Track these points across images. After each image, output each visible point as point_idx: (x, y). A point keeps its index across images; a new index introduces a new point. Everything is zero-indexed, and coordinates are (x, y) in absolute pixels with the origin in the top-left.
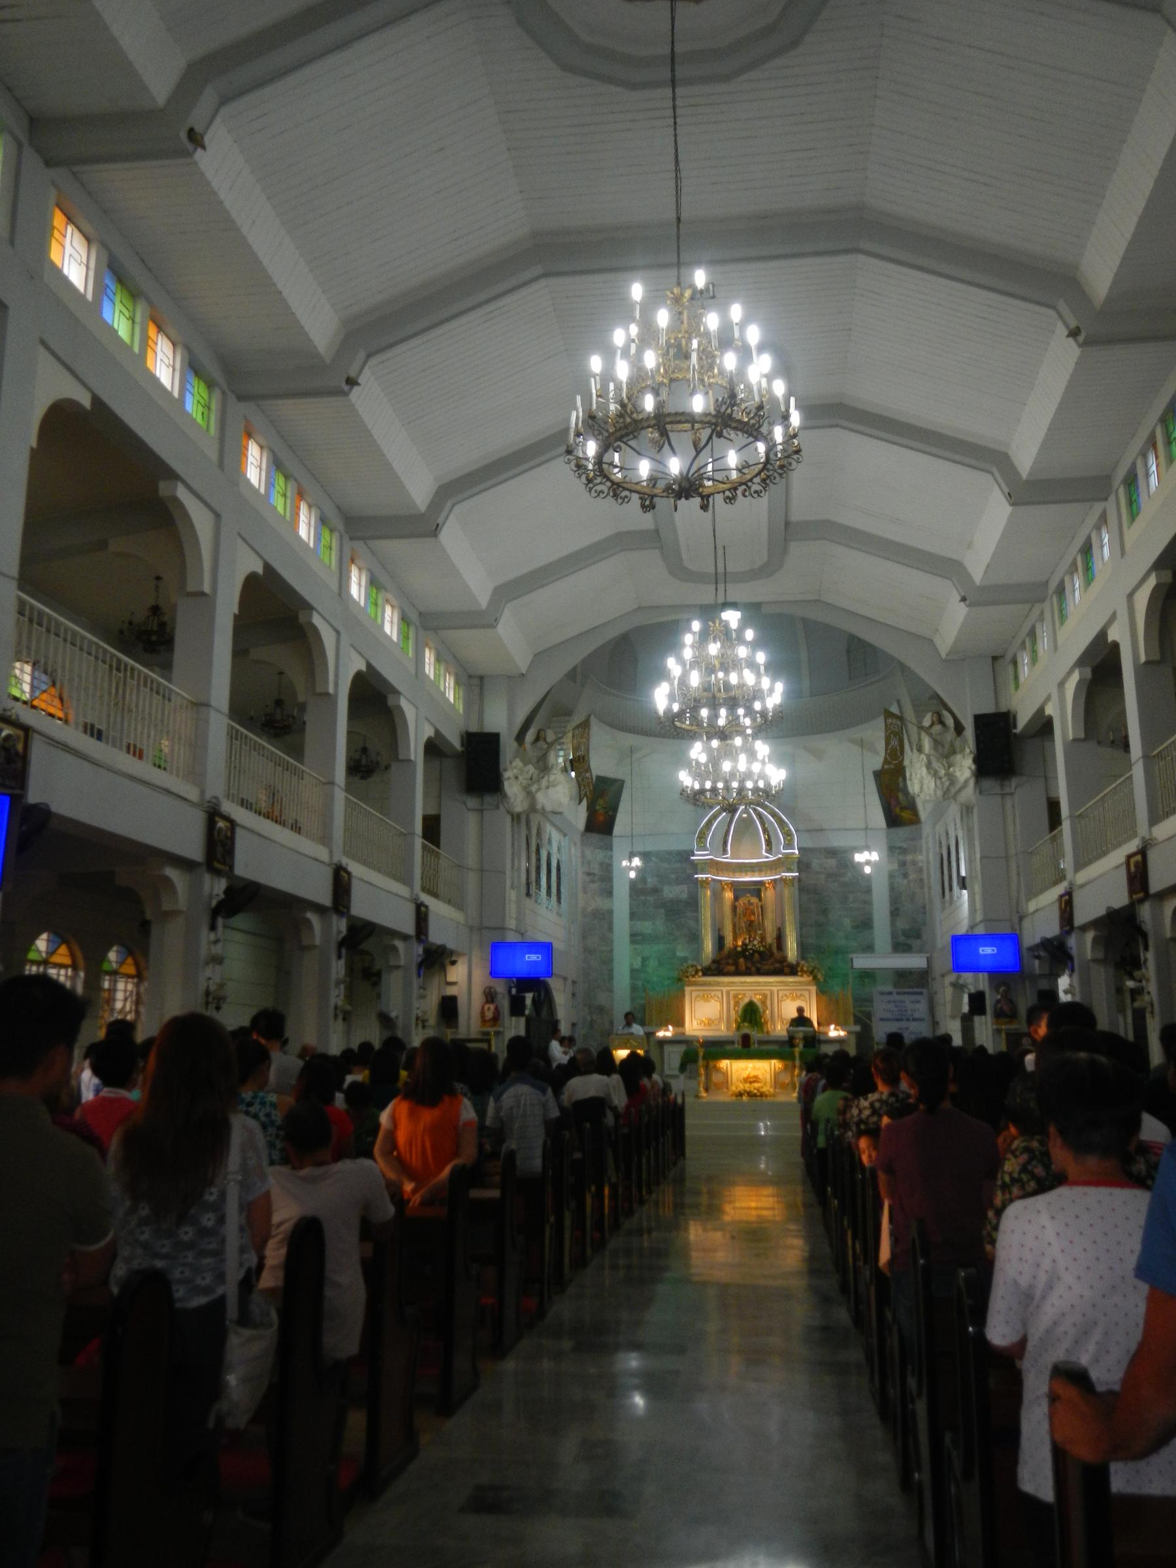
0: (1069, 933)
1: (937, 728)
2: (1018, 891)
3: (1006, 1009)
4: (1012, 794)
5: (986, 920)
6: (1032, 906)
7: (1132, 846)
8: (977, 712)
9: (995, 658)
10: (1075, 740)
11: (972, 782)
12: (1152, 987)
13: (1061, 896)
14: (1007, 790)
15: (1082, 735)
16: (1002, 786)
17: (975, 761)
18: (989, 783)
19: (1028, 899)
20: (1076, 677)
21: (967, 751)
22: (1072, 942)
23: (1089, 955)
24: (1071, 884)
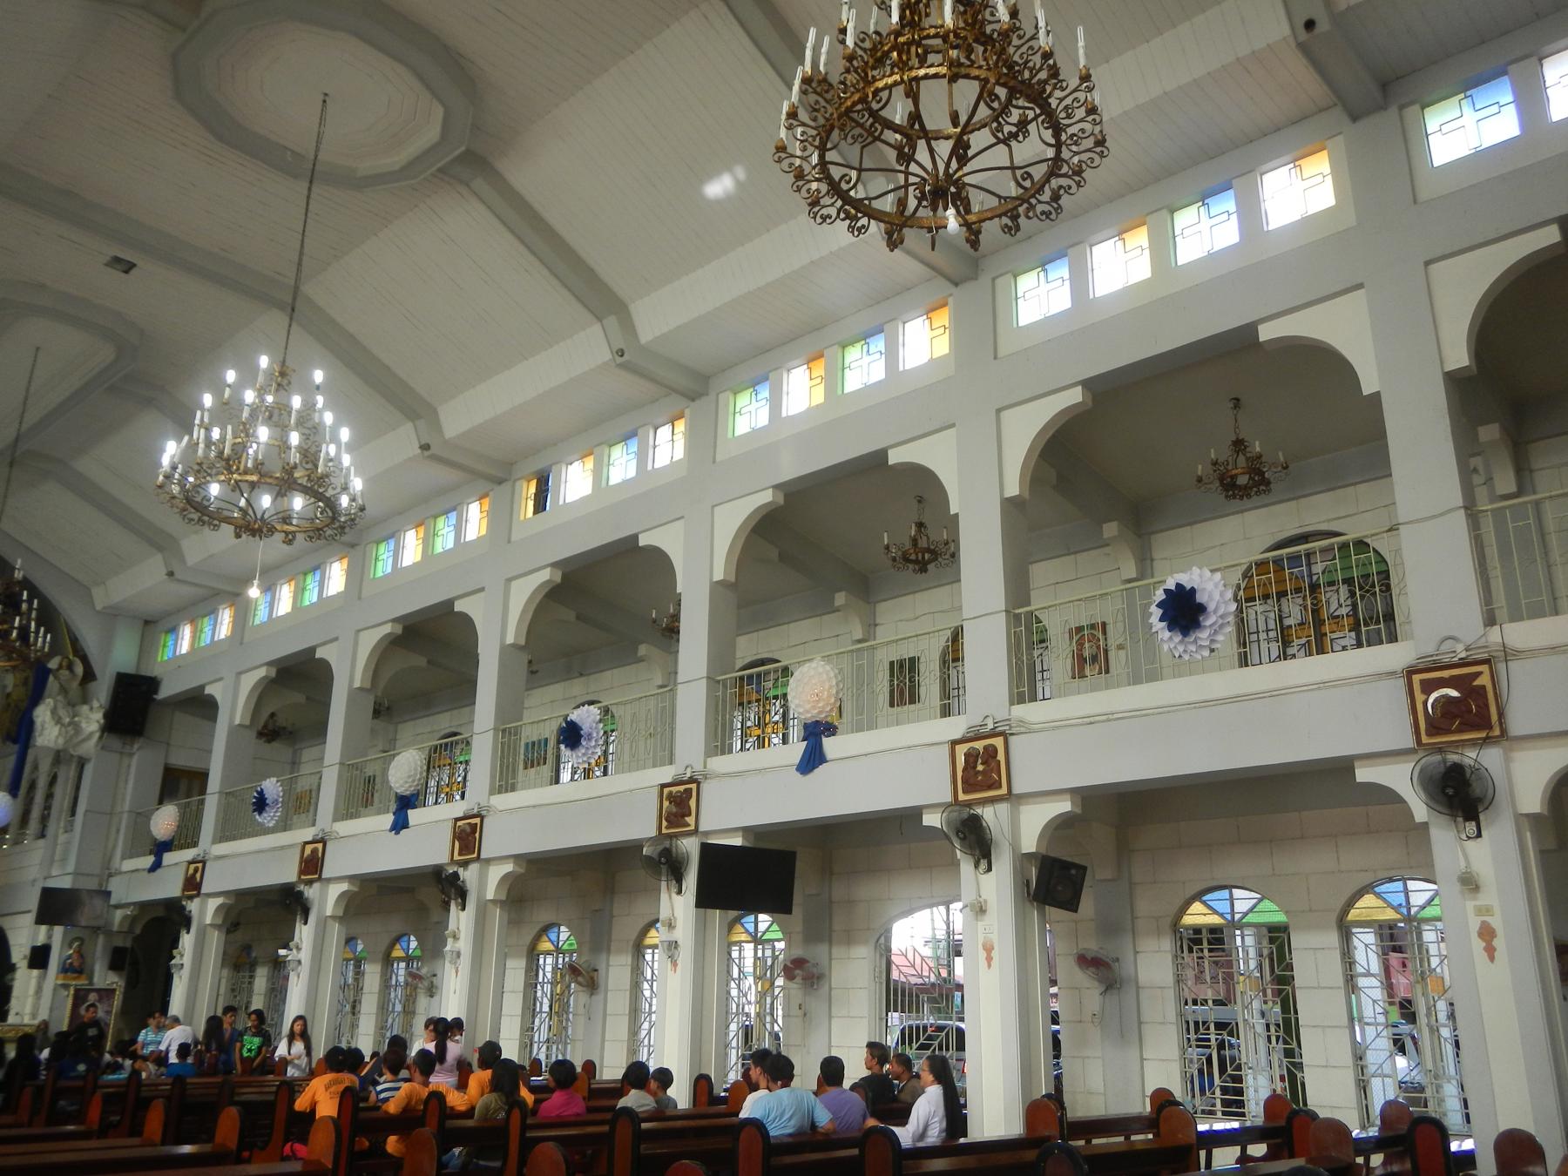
0: (191, 898)
1: (65, 673)
2: (114, 847)
3: (76, 964)
4: (131, 755)
5: (76, 874)
6: (128, 865)
7: (308, 834)
8: (123, 671)
9: (147, 622)
11: (97, 735)
12: (305, 955)
13: (190, 863)
15: (248, 722)
17: (106, 716)
18: (115, 742)
19: (123, 858)
20: (262, 672)
21: (96, 704)
22: (193, 906)
23: (208, 921)
24: (205, 853)
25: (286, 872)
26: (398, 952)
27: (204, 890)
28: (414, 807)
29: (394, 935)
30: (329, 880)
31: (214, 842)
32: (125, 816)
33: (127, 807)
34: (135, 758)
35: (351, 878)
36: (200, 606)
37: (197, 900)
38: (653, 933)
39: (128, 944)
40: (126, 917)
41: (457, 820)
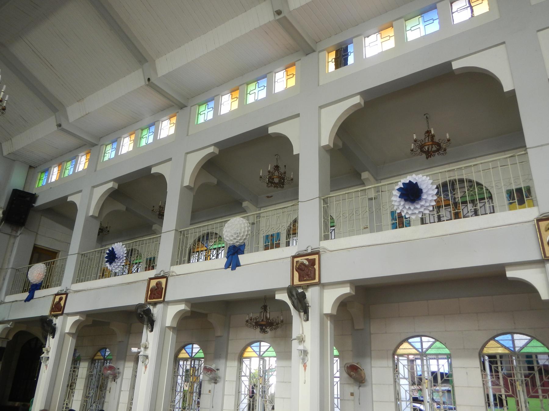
0: (56, 316)
4: (15, 237)
9: (31, 167)
10: (92, 216)
12: (152, 352)
13: (57, 294)
14: (14, 233)
16: (12, 230)
19: (6, 294)
20: (110, 185)
22: (57, 321)
23: (67, 330)
25: (137, 297)
26: (183, 354)
27: (66, 311)
28: (243, 253)
29: (183, 344)
30: (169, 303)
31: (73, 283)
32: (9, 271)
33: (10, 266)
34: (18, 240)
35: (187, 301)
36: (67, 155)
37: (60, 318)
38: (405, 345)
39: (5, 345)
40: (6, 328)
41: (294, 257)
